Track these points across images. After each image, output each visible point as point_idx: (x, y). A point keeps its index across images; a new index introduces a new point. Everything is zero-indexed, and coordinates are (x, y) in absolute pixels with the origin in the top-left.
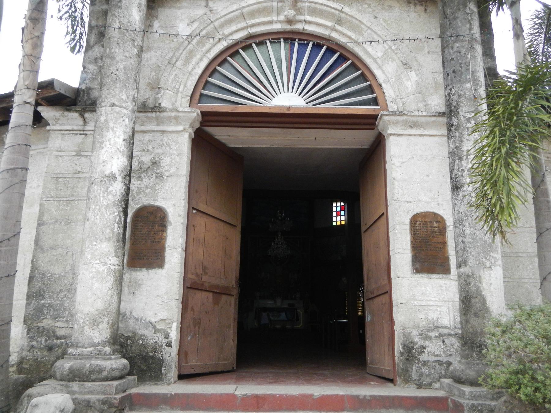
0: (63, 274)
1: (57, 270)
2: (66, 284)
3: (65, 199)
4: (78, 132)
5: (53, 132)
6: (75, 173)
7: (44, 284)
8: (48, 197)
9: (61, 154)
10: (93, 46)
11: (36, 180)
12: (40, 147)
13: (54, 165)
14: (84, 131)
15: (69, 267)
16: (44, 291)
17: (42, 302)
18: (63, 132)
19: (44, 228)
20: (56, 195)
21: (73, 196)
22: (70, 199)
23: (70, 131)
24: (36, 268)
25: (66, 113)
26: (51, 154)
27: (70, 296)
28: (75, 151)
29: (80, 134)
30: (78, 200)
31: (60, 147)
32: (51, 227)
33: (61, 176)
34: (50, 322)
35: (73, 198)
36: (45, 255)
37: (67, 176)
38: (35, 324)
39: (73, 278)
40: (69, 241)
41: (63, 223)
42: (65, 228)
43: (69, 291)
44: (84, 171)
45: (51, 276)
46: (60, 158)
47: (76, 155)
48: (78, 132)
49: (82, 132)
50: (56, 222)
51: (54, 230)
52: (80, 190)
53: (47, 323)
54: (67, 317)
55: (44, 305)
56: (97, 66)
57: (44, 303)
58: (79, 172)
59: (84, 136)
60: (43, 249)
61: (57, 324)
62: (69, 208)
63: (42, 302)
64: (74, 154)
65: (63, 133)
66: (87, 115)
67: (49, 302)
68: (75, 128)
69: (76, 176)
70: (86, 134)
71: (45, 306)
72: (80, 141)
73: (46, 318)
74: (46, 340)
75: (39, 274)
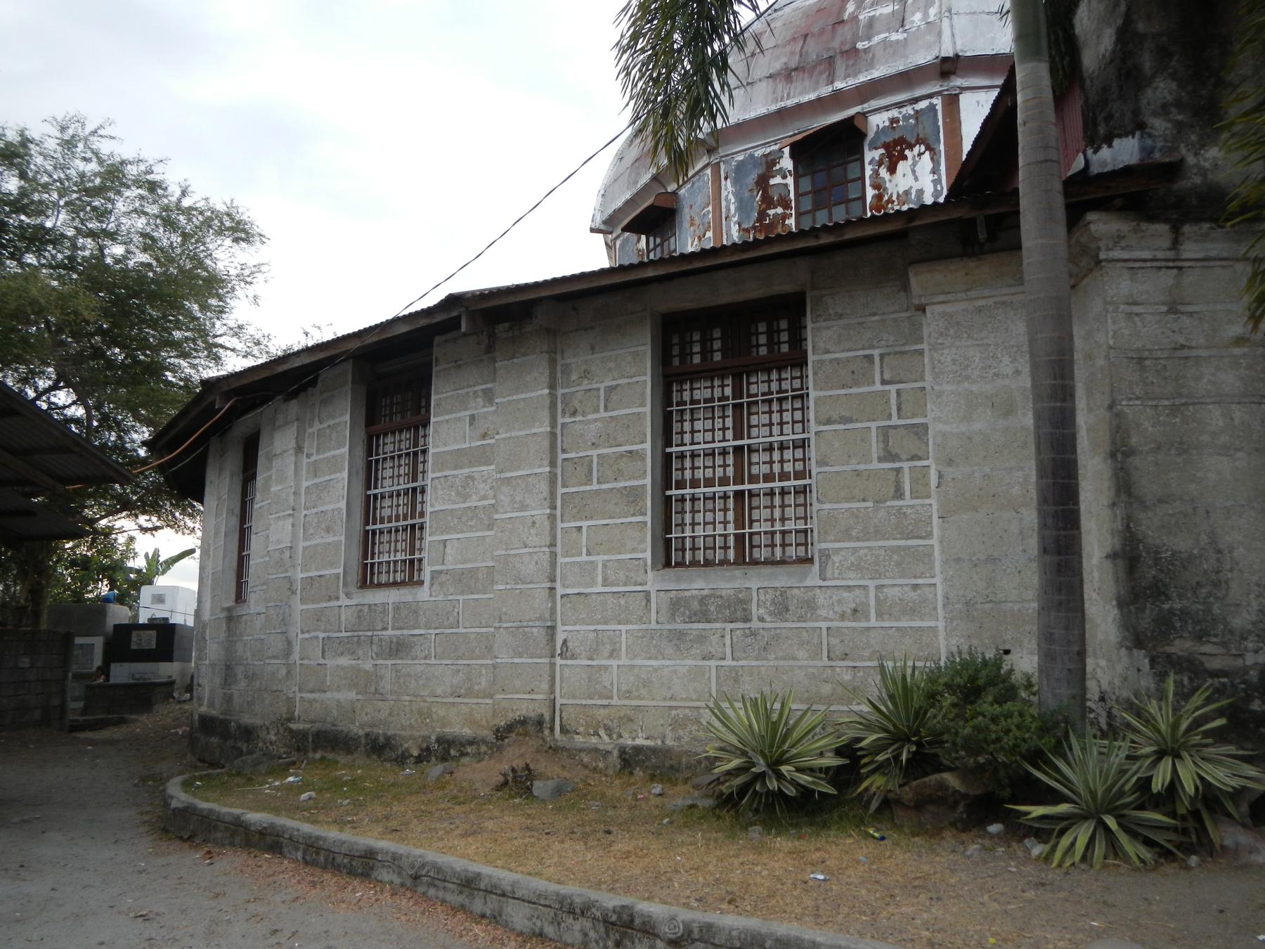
0: (1195, 551)
1: (1182, 543)
2: (1206, 572)
3: (1166, 403)
4: (1163, 264)
5: (1110, 265)
6: (1175, 349)
7: (1162, 571)
8: (1130, 399)
9: (1136, 309)
10: (1153, 76)
11: (1006, 360)
12: (1005, 291)
13: (1127, 332)
14: (1174, 260)
15: (1204, 538)
16: (1165, 585)
17: (1166, 606)
18: (1131, 265)
19: (1136, 461)
20: (1147, 393)
21: (1180, 395)
22: (1177, 401)
23: (1145, 261)
24: (1140, 541)
25: (1144, 226)
26: (1116, 311)
27: (1219, 595)
28: (1163, 304)
29: (1168, 268)
30: (1194, 404)
31: (1132, 296)
32: (1150, 458)
33: (1146, 354)
34: (1188, 644)
35: (1183, 401)
36: (1150, 514)
37: (1159, 354)
38: (1161, 650)
39: (1218, 560)
40: (1192, 487)
41: (1173, 452)
42: (1179, 460)
43: (1216, 584)
44: (1193, 344)
45: (1173, 555)
46: (1137, 319)
47: (1168, 312)
48: (1163, 264)
49: (1171, 264)
50: (1159, 448)
51: (1157, 464)
52: (1192, 384)
53: (1180, 646)
54: (1224, 635)
55: (1171, 612)
56: (1170, 121)
57: (1171, 608)
58: (1183, 347)
59: (1175, 271)
60: (1143, 502)
61: (1207, 648)
62: (1178, 420)
63: (1166, 606)
64: (1164, 308)
65: (1133, 267)
66: (1187, 229)
67: (1179, 606)
68: (1160, 255)
69: (1178, 354)
70: (1180, 268)
71: (1175, 615)
72: (1171, 281)
73: (1181, 637)
74: (1191, 679)
75: (1148, 553)
